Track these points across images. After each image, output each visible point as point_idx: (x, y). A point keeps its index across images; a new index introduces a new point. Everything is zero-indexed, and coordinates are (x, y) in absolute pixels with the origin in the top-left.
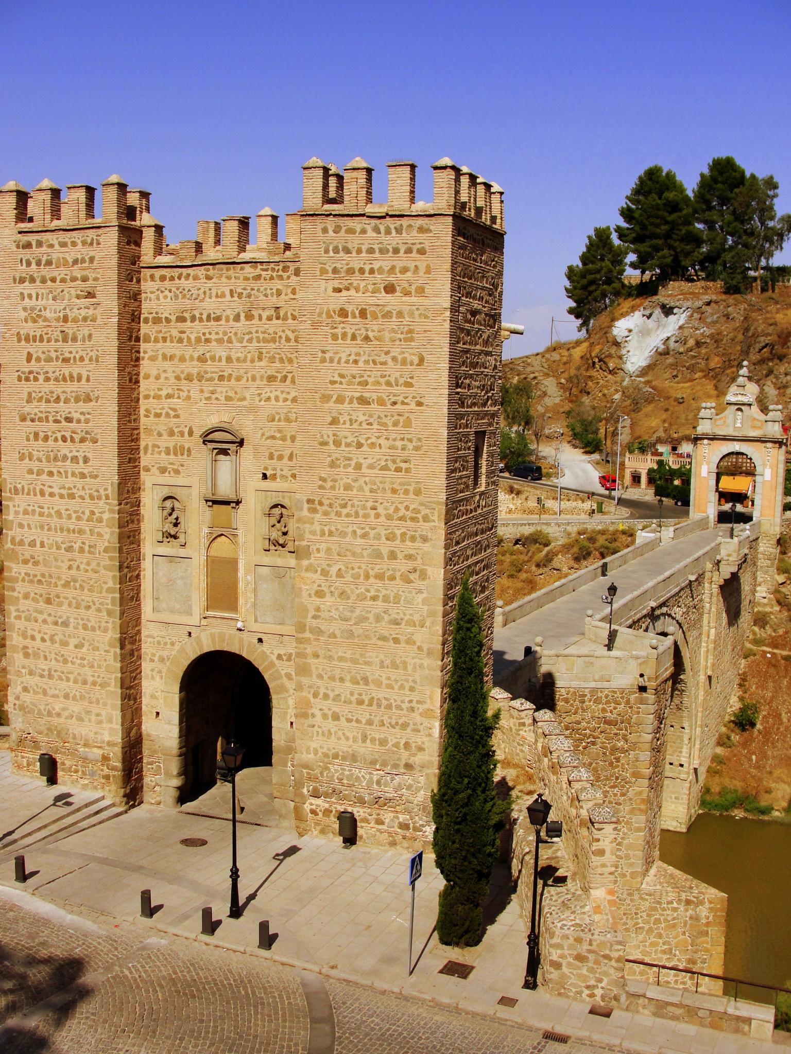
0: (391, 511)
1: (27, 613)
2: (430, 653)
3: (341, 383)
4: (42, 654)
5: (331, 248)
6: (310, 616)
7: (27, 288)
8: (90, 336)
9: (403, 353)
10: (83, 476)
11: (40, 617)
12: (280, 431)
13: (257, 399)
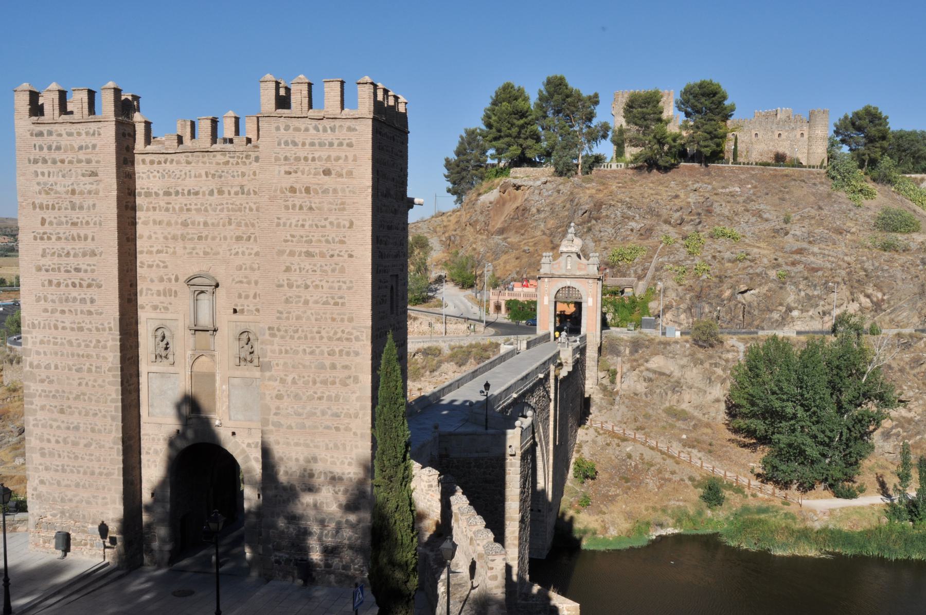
0: (331, 335)
1: (44, 421)
2: (363, 436)
3: (292, 241)
4: (56, 453)
5: (282, 142)
6: (272, 413)
7: (40, 167)
8: (94, 205)
9: (338, 219)
10: (90, 313)
11: (55, 424)
12: (246, 277)
13: (228, 253)
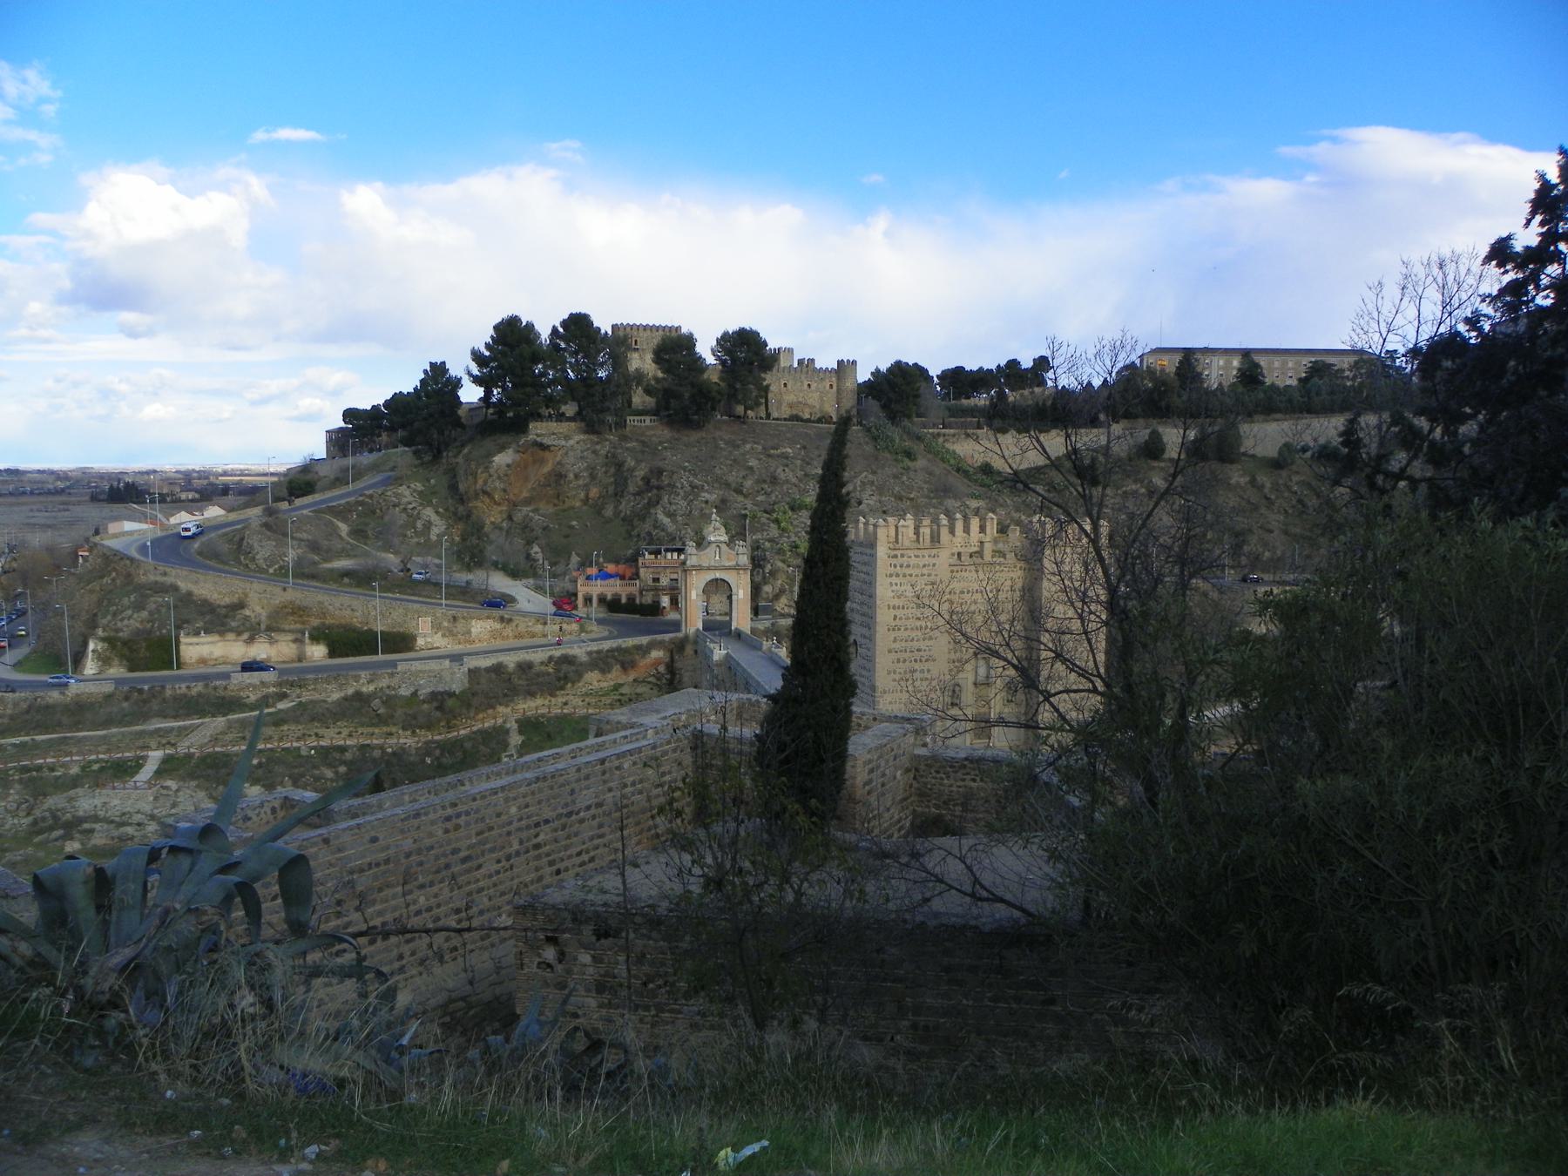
7: (894, 580)
